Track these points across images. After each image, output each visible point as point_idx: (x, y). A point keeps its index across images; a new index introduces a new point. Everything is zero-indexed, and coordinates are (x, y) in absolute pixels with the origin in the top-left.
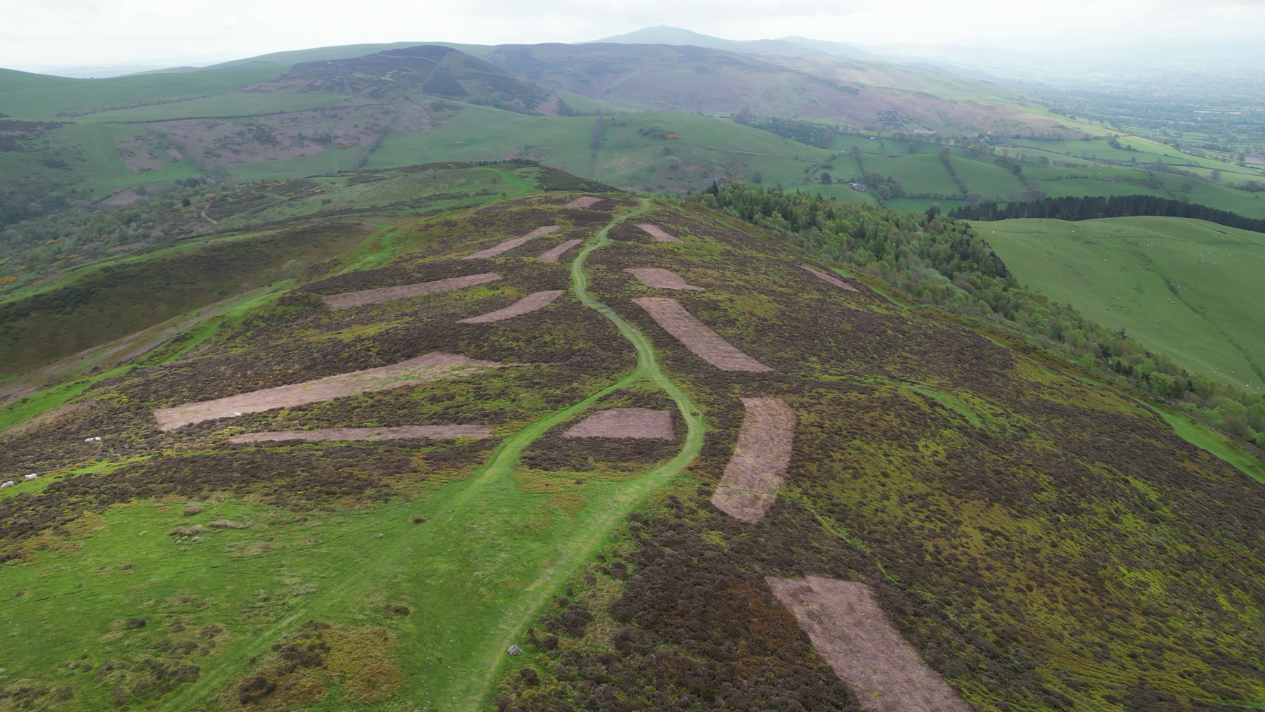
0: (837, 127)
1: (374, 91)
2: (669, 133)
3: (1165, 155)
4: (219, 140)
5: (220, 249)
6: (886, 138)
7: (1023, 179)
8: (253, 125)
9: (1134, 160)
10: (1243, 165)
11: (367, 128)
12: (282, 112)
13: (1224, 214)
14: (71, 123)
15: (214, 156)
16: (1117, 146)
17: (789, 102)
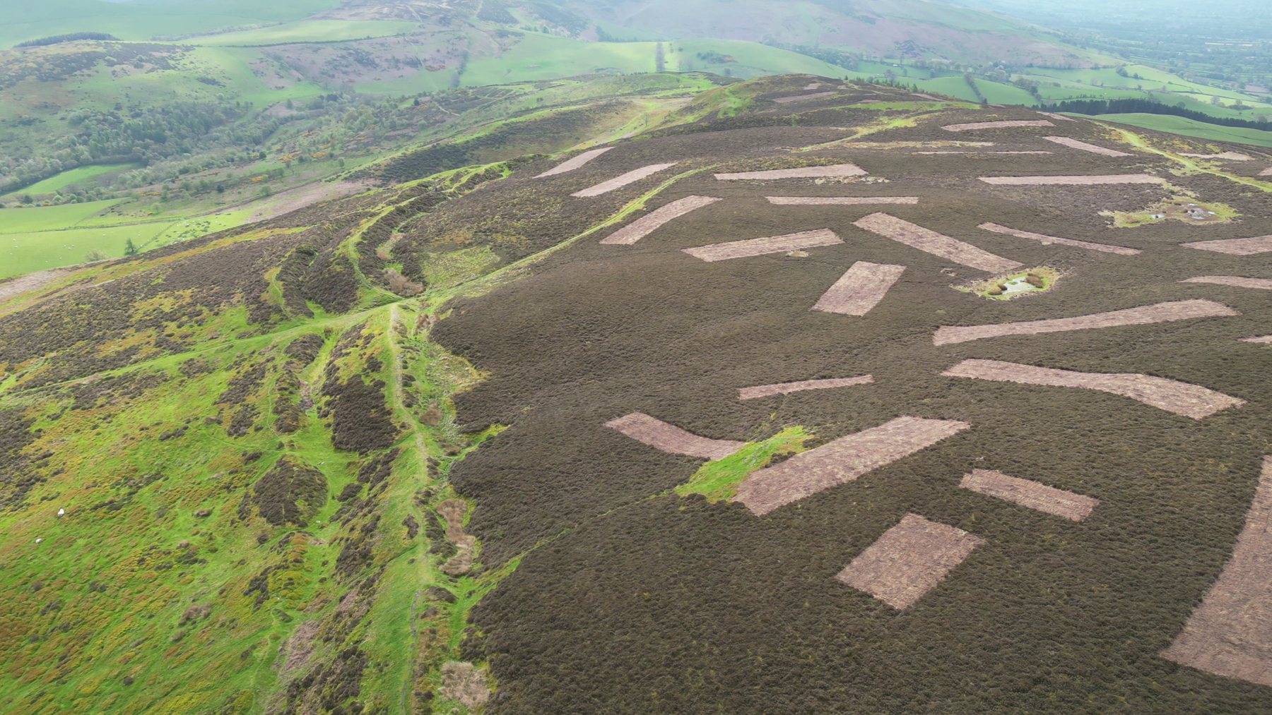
0: (862, 56)
1: (443, 19)
2: (725, 56)
3: (1170, 83)
4: (330, 63)
5: (565, 114)
6: (908, 66)
7: (1039, 98)
8: (349, 49)
9: (1140, 88)
10: (1242, 93)
11: (448, 53)
12: (368, 38)
13: (1197, 113)
14: (198, 46)
15: (330, 76)
16: (1125, 75)
17: (809, 31)
